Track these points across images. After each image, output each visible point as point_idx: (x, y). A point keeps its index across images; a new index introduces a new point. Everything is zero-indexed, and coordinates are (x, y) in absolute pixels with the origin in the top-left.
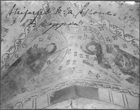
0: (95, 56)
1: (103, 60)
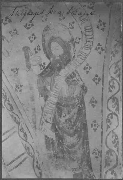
0: (47, 62)
1: (48, 79)
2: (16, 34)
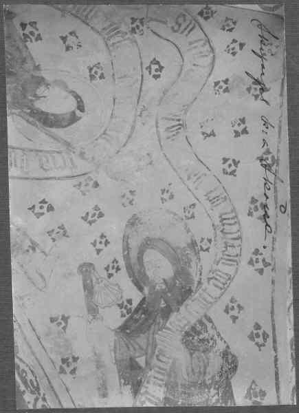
0: (136, 297)
1: (142, 340)
2: (64, 235)
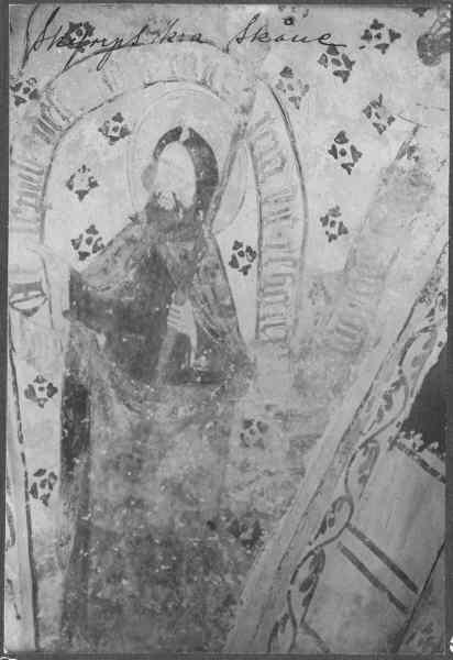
2: (380, 104)
